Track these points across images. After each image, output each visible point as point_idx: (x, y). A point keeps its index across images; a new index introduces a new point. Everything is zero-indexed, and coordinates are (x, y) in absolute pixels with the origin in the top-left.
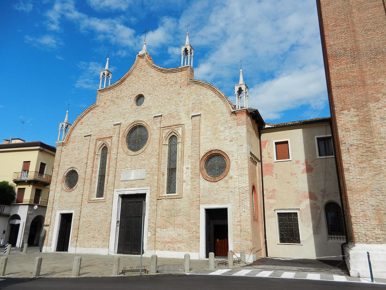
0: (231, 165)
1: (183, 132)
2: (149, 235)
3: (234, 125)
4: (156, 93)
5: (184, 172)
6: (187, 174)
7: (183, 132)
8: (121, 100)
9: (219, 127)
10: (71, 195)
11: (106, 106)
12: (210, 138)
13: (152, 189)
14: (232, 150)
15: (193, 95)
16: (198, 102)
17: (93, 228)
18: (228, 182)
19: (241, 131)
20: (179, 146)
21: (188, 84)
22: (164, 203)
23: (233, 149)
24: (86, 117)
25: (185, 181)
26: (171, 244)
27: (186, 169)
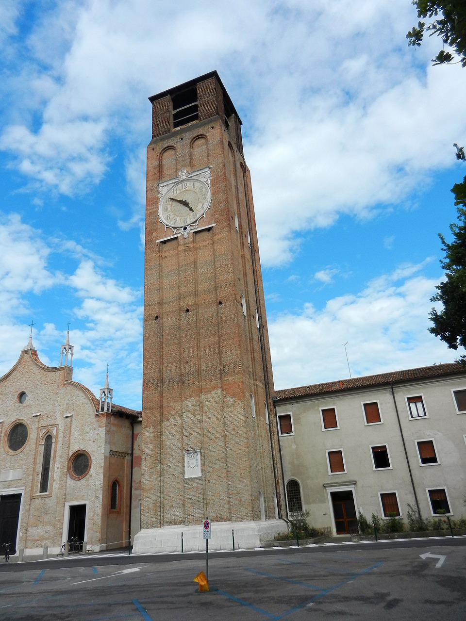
2: (21, 534)
20: (53, 446)
21: (64, 385)
25: (54, 481)
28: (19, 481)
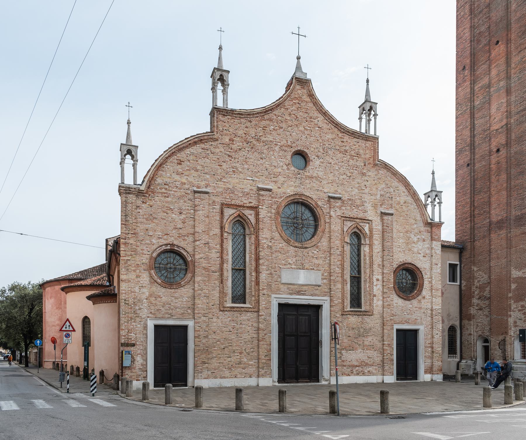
1: (371, 230)
4: (327, 158)
5: (375, 284)
6: (378, 287)
7: (371, 230)
8: (266, 147)
9: (412, 236)
10: (176, 295)
11: (234, 147)
12: (403, 247)
13: (334, 300)
14: (425, 267)
15: (381, 182)
16: (388, 195)
17: (237, 350)
19: (437, 248)
22: (350, 320)
23: (426, 266)
24: (189, 153)
25: (375, 296)
26: (360, 368)
27: (376, 281)
28: (316, 288)
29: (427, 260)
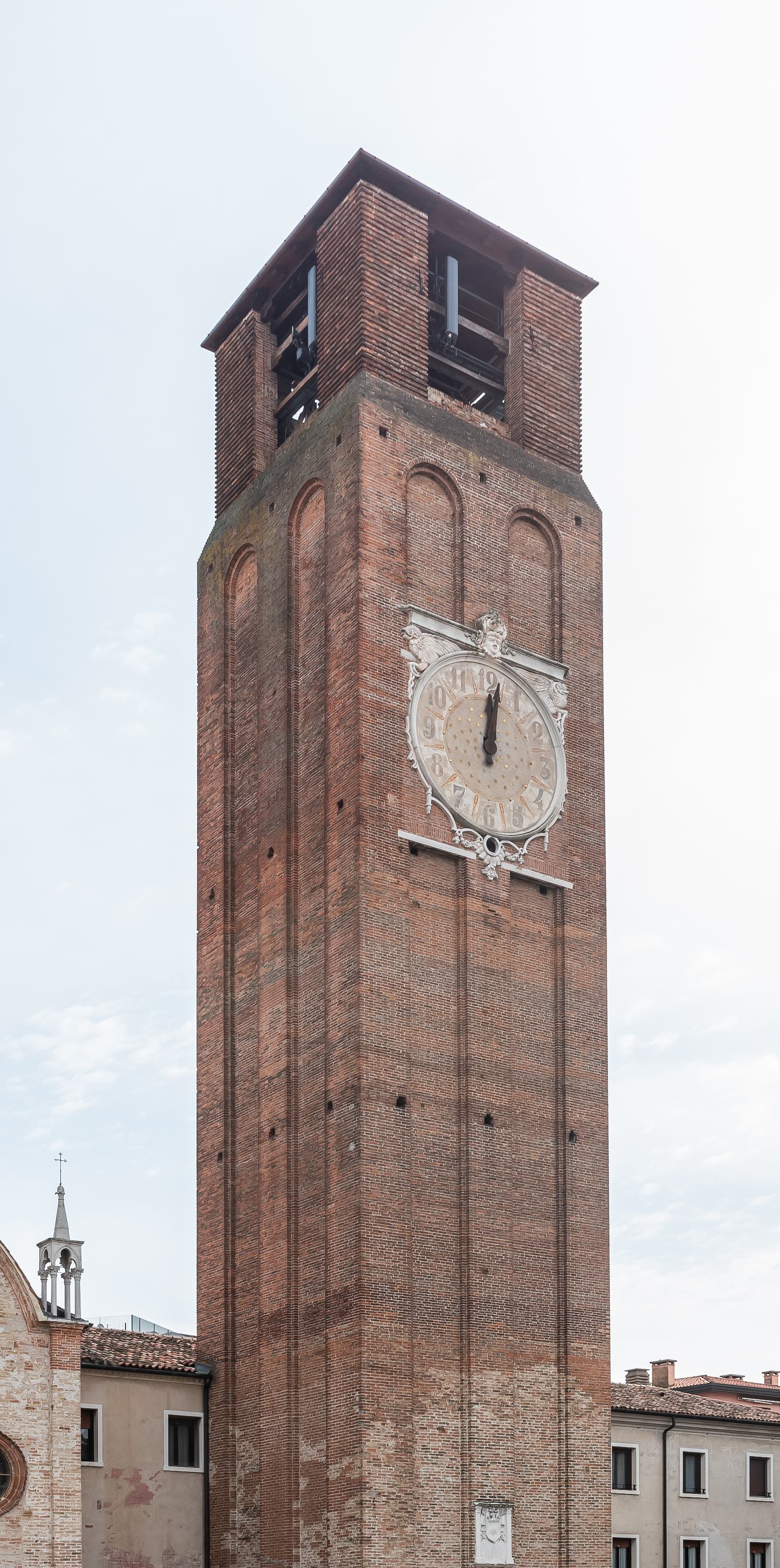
0: (29, 1477)
3: (38, 1360)
14: (33, 1435)
18: (19, 1526)
19: (67, 1387)
23: (35, 1433)
29: (39, 1418)
